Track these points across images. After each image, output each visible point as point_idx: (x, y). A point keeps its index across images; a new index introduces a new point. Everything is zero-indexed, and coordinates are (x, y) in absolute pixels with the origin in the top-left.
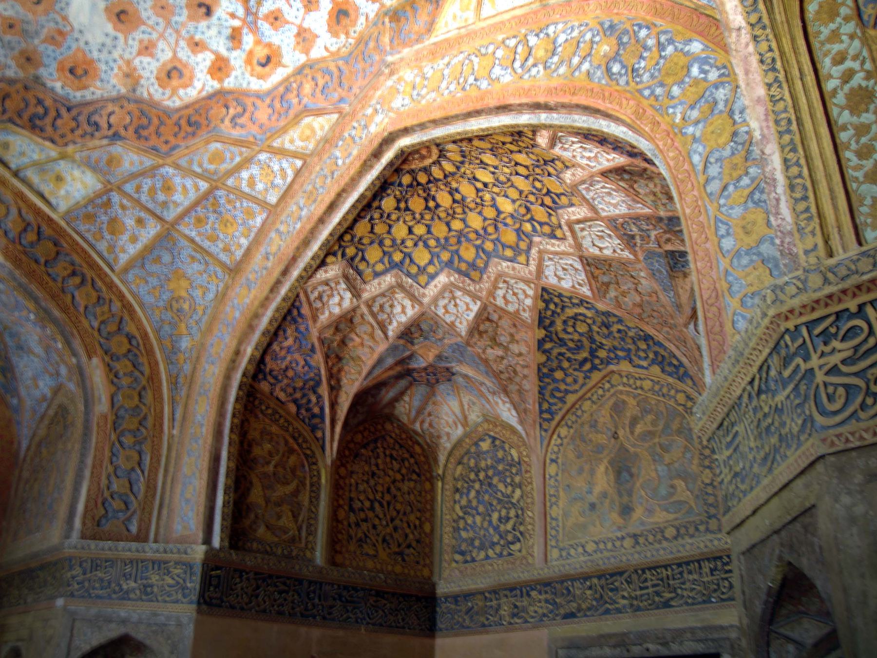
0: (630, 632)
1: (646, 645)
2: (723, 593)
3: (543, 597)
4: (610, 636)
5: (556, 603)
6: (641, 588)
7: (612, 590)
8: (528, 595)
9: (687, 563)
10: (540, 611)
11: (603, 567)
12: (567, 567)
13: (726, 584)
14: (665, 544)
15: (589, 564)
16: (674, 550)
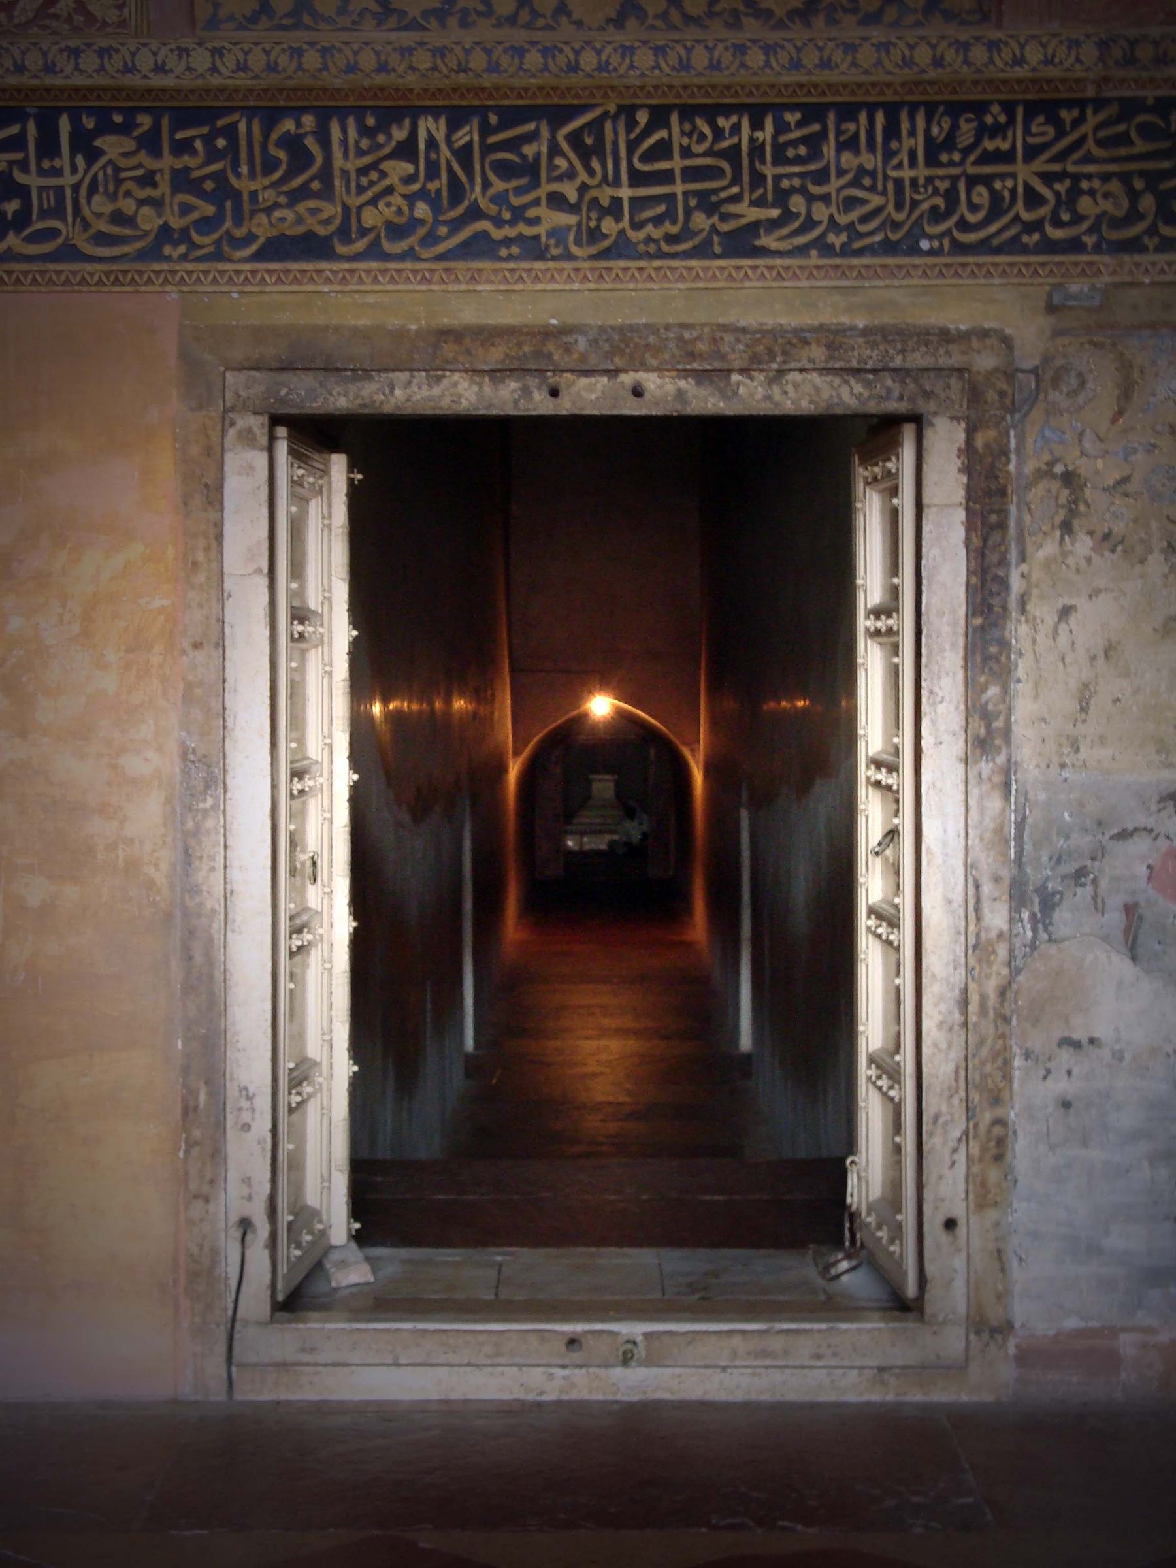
0: (565, 330)
1: (627, 379)
2: (963, 225)
3: (168, 161)
4: (487, 335)
5: (236, 195)
6: (637, 179)
7: (505, 170)
8: (84, 144)
9: (848, 112)
10: (148, 220)
11: (488, 81)
12: (312, 59)
13: (981, 195)
14: (752, 28)
15: (423, 61)
16: (811, 58)
